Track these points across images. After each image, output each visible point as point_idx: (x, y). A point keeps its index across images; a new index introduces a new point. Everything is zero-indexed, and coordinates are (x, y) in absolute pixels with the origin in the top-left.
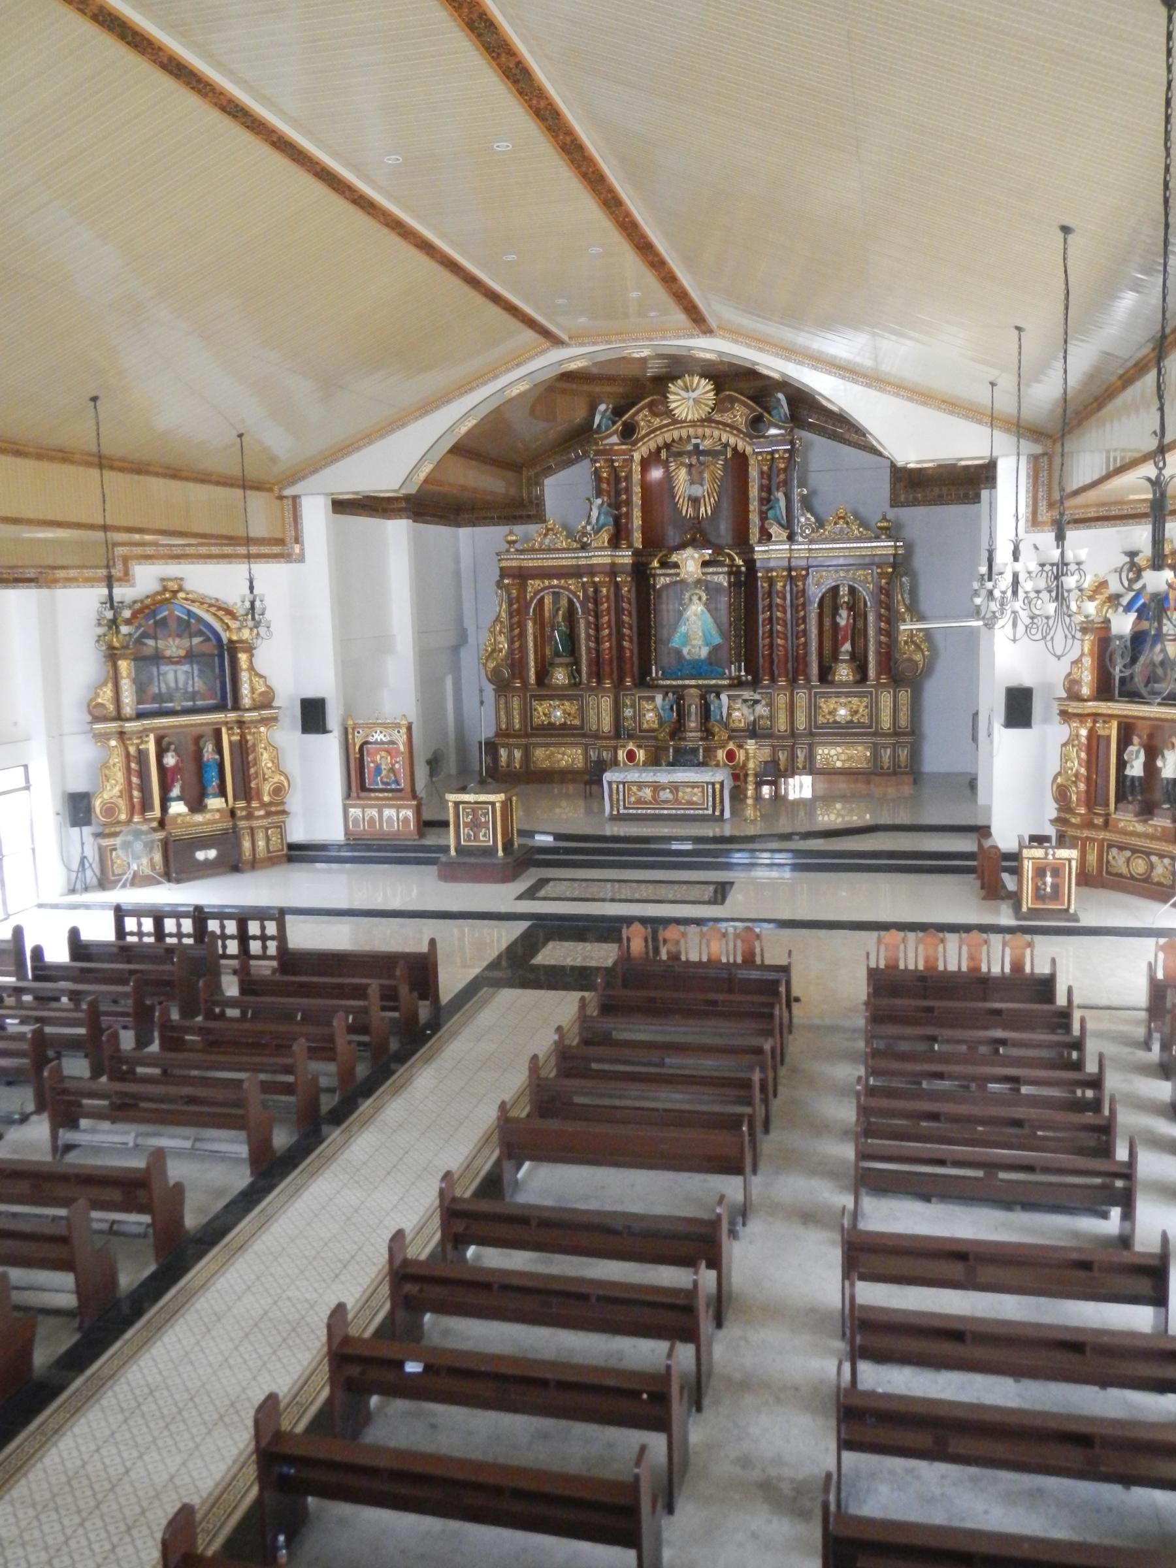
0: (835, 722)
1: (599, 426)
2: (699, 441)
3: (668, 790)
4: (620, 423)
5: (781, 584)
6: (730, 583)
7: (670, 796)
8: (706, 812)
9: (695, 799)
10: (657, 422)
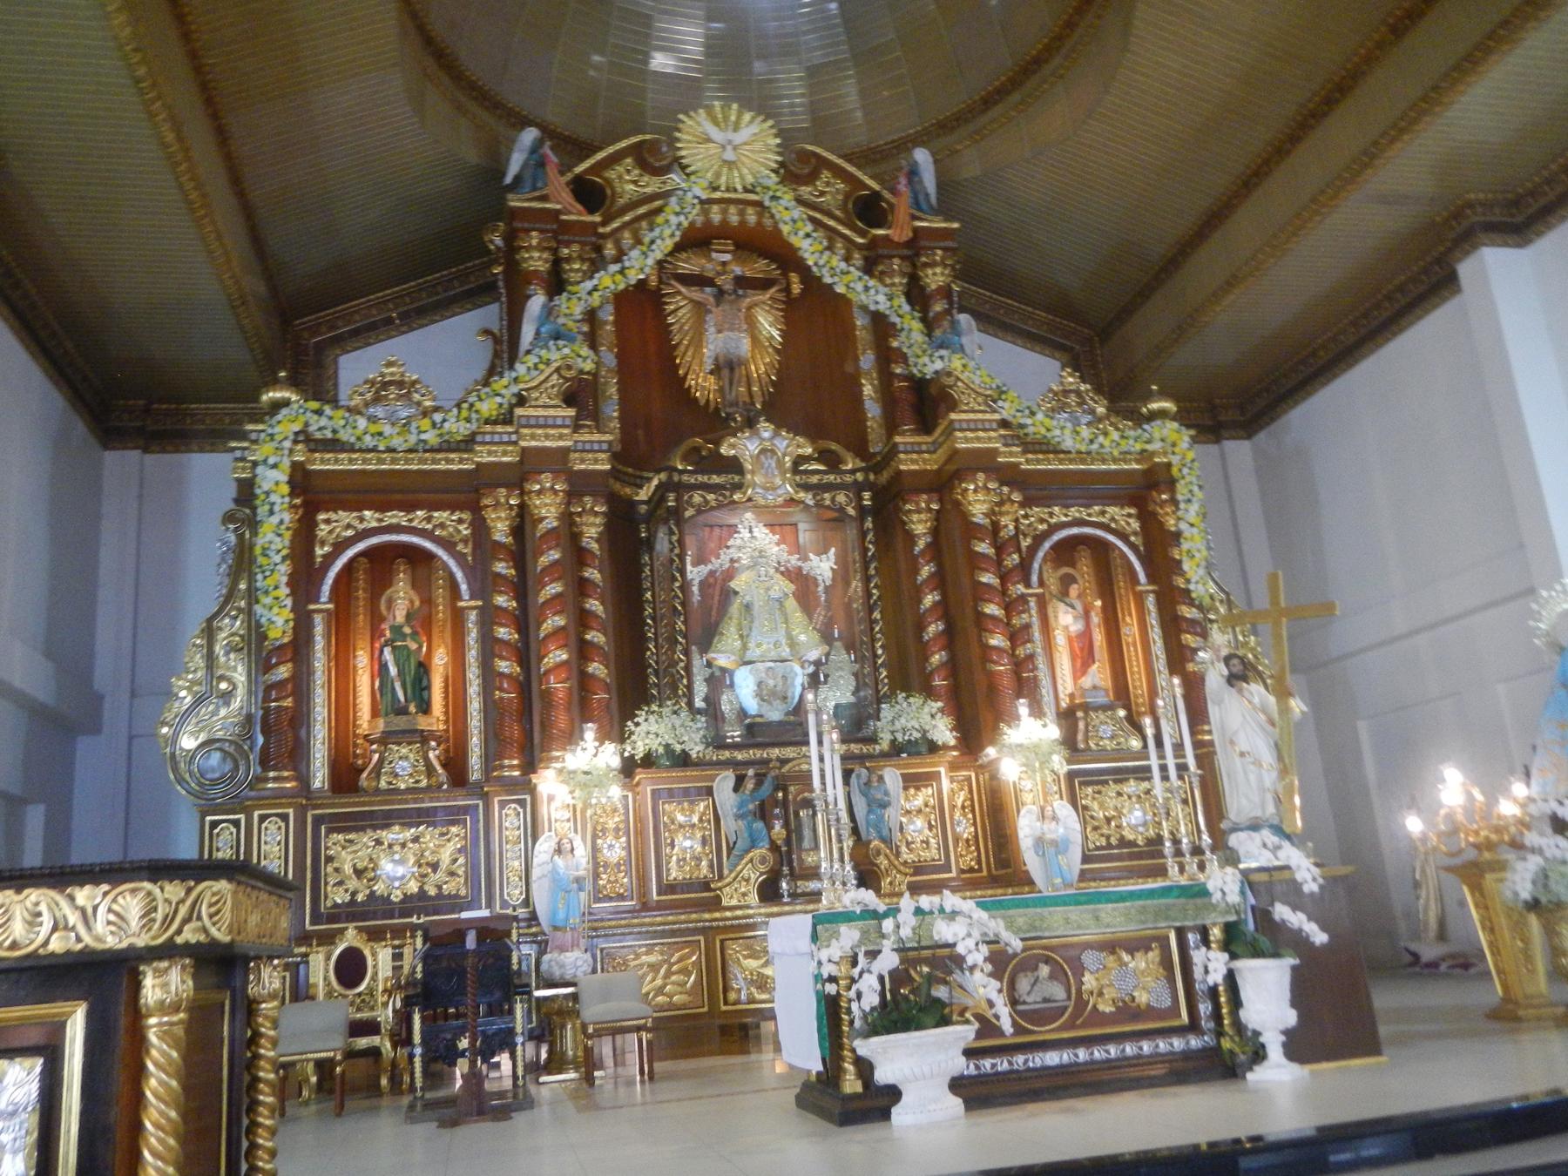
0: (1123, 843)
1: (518, 179)
2: (727, 257)
3: (1045, 970)
4: (569, 176)
5: (984, 508)
6: (862, 510)
7: (1058, 992)
8: (1195, 1042)
9: (1142, 998)
10: (652, 185)
